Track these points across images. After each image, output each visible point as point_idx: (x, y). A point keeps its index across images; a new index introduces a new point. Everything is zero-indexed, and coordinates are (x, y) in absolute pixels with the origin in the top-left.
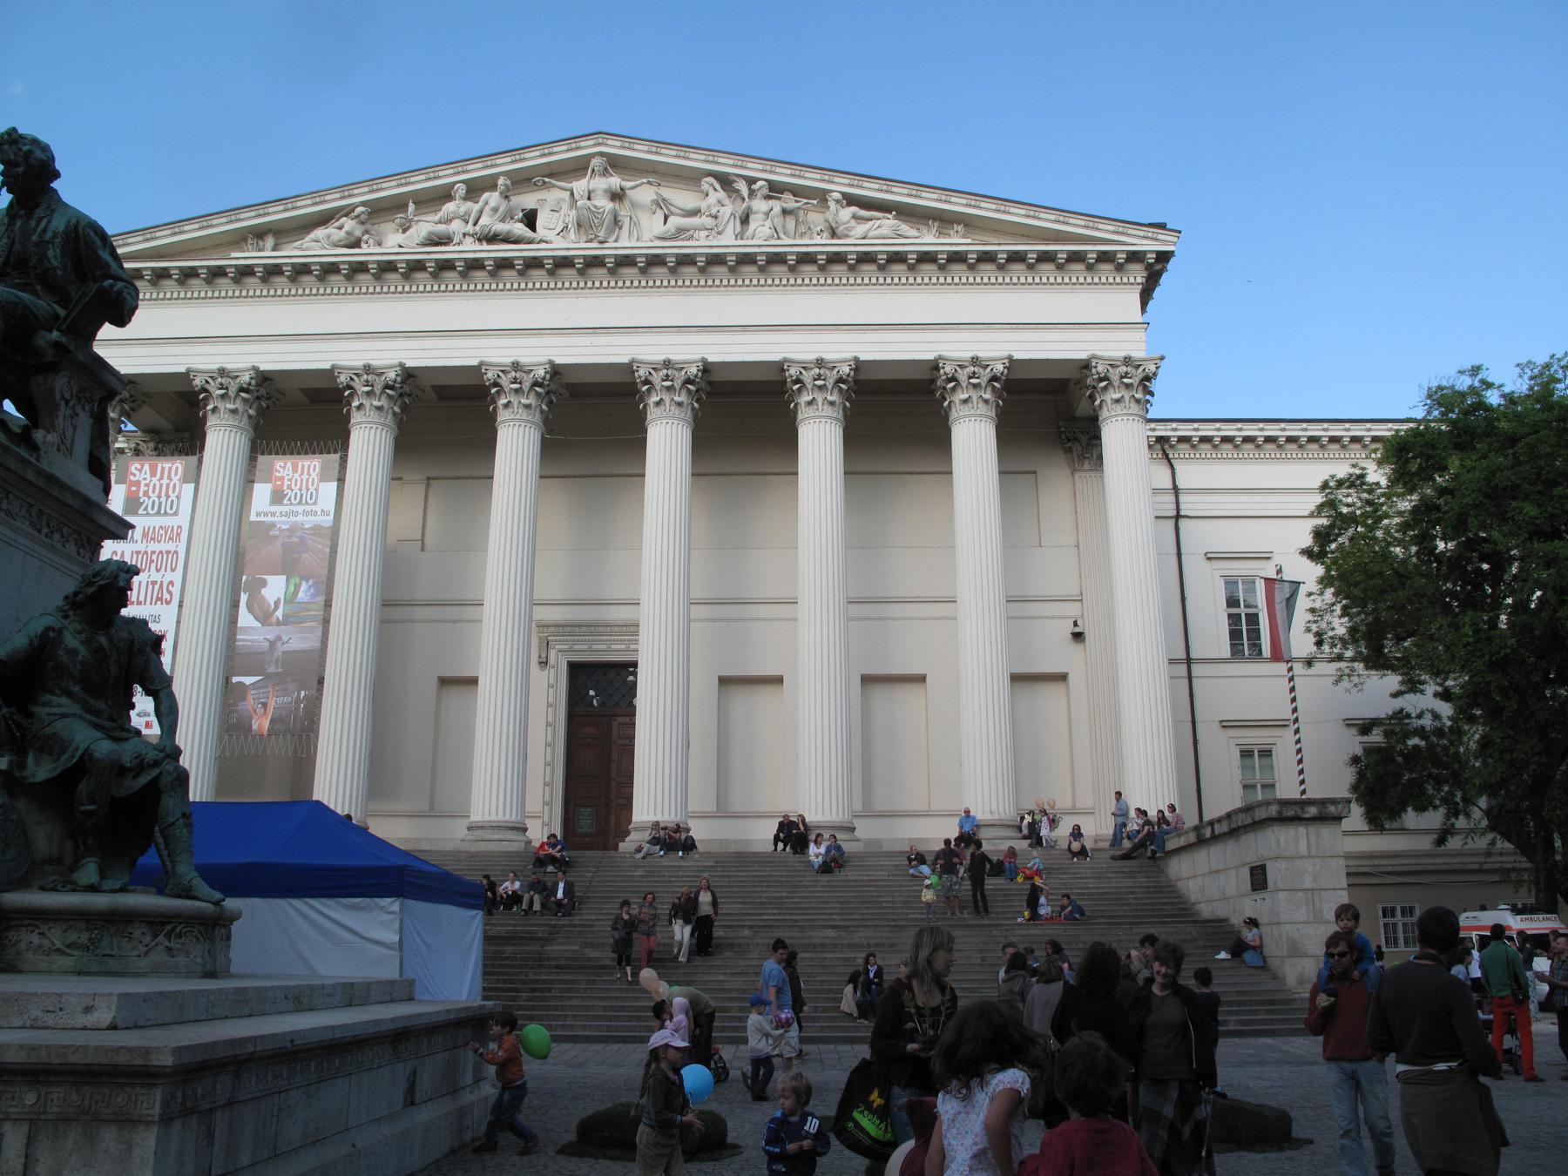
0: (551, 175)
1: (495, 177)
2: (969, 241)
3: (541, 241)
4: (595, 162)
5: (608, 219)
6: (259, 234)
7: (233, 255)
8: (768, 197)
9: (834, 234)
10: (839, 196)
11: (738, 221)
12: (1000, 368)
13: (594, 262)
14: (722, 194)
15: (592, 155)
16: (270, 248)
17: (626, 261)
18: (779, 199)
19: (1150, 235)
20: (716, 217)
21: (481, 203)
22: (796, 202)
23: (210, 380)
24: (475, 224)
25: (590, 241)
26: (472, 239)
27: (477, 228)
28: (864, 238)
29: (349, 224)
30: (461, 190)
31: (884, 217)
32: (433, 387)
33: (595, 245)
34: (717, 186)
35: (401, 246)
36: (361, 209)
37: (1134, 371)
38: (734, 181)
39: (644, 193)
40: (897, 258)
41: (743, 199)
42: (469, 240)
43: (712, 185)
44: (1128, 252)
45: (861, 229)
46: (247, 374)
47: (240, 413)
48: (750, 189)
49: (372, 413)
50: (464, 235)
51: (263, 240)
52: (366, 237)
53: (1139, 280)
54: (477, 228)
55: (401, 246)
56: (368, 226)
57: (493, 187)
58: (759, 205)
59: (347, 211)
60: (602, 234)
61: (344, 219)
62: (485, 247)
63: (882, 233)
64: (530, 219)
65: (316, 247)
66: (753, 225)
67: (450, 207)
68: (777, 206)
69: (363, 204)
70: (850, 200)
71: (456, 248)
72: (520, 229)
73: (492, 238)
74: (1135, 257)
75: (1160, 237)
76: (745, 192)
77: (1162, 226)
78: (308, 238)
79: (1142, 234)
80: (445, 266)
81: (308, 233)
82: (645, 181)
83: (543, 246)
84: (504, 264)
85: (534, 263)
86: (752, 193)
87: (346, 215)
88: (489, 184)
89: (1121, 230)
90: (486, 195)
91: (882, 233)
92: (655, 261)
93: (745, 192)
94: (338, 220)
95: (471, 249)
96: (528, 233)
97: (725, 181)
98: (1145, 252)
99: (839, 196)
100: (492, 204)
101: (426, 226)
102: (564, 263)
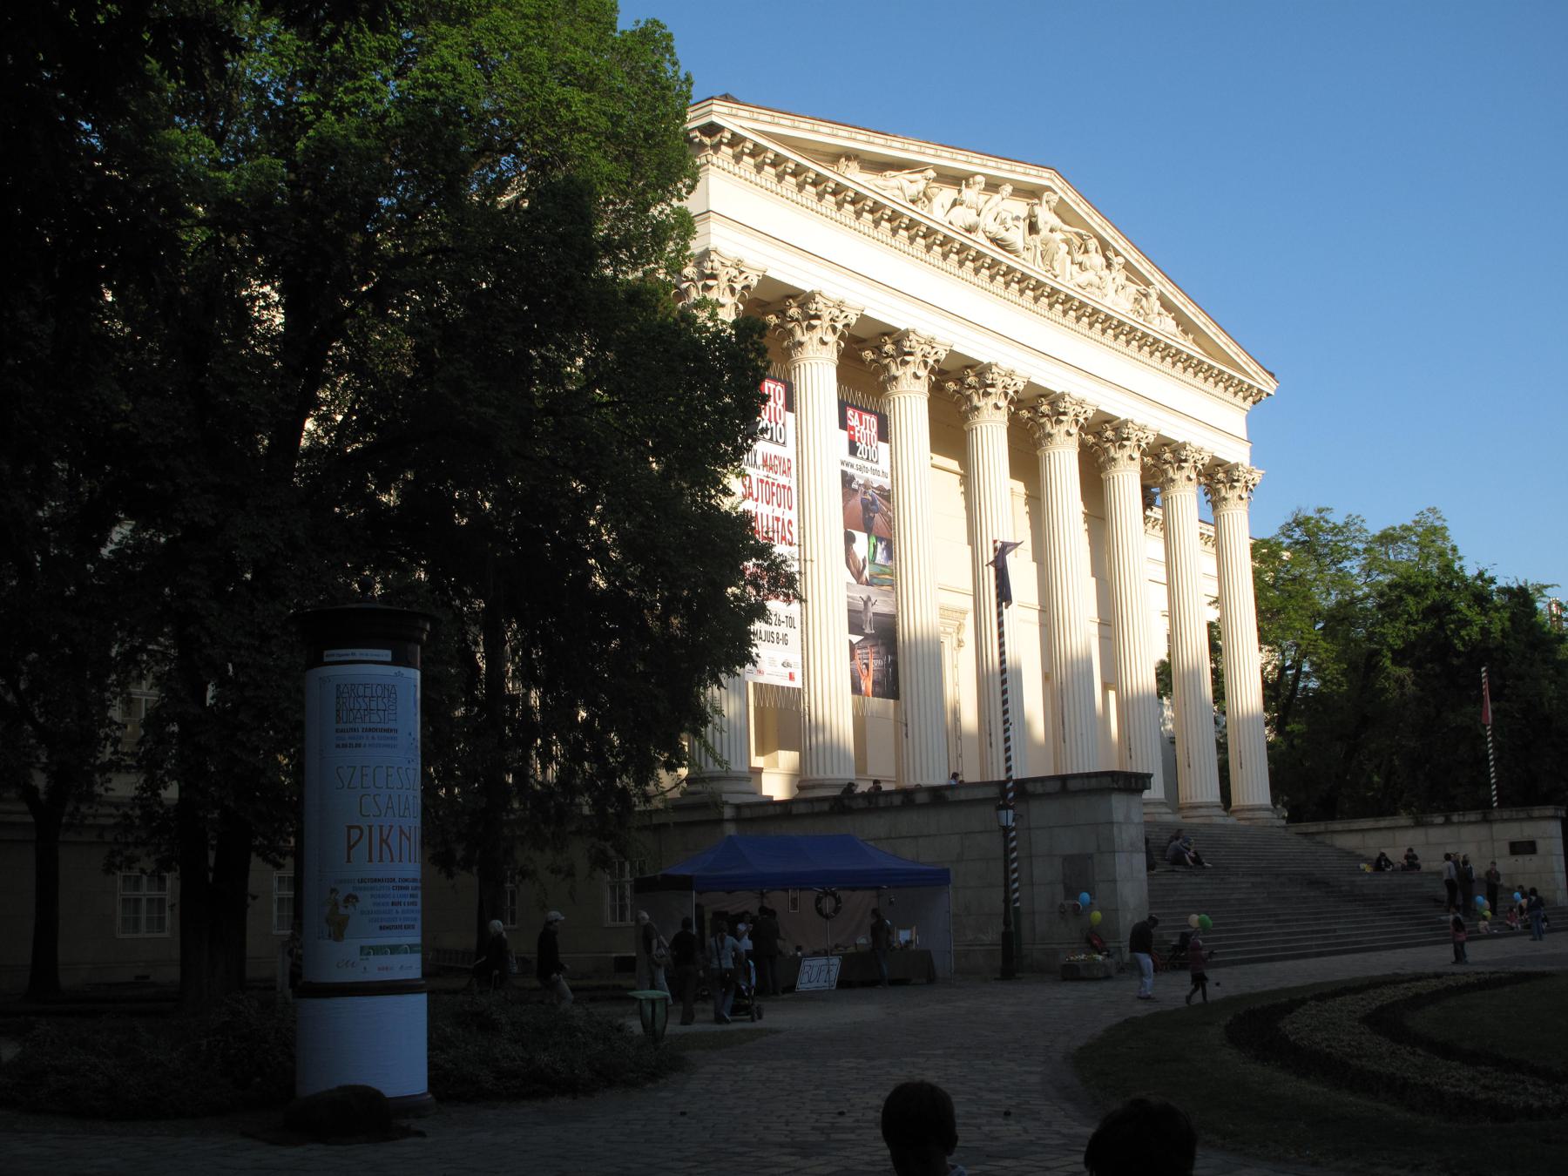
35: (950, 223)
55: (950, 223)
63: (1165, 327)
65: (892, 189)
69: (936, 168)
77: (1272, 375)
78: (894, 183)
91: (1165, 327)
97: (1104, 246)
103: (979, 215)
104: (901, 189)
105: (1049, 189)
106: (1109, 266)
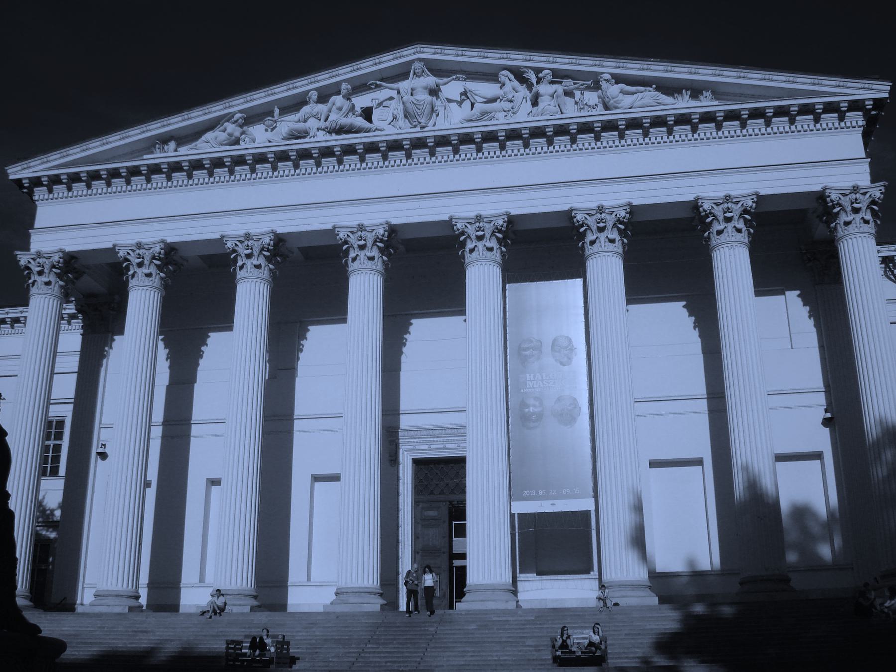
0: (382, 80)
1: (339, 84)
2: (716, 103)
3: (376, 129)
4: (417, 65)
5: (428, 109)
6: (164, 140)
7: (145, 157)
8: (552, 82)
9: (607, 107)
10: (608, 76)
11: (529, 102)
12: (750, 203)
13: (419, 144)
14: (516, 83)
15: (413, 61)
16: (172, 150)
17: (443, 141)
18: (561, 83)
19: (866, 86)
20: (511, 101)
21: (329, 104)
22: (575, 83)
23: (131, 252)
24: (326, 120)
25: (415, 127)
26: (324, 133)
27: (327, 124)
28: (630, 108)
29: (230, 127)
30: (314, 95)
31: (645, 90)
32: (301, 249)
33: (418, 129)
34: (512, 77)
35: (270, 142)
36: (238, 116)
37: (862, 197)
38: (525, 72)
39: (453, 88)
40: (659, 122)
41: (533, 85)
42: (321, 133)
43: (507, 76)
44: (850, 101)
45: (628, 100)
46: (158, 245)
47: (154, 276)
48: (537, 77)
49: (252, 270)
50: (318, 130)
51: (167, 145)
52: (244, 136)
53: (861, 123)
54: (327, 124)
55: (270, 142)
56: (245, 128)
57: (338, 93)
58: (544, 89)
59: (228, 118)
60: (422, 121)
61: (227, 124)
62: (334, 137)
64: (367, 114)
66: (541, 105)
67: (305, 109)
68: (559, 88)
69: (240, 111)
70: (618, 79)
71: (312, 140)
72: (360, 122)
73: (341, 130)
74: (855, 105)
75: (874, 86)
76: (534, 80)
79: (859, 85)
80: (305, 154)
81: (200, 137)
82: (454, 77)
83: (378, 133)
84: (350, 150)
85: (372, 148)
86: (539, 81)
87: (228, 121)
88: (335, 89)
89: (842, 83)
90: (333, 98)
92: (467, 139)
93: (534, 80)
94: (222, 126)
95: (322, 139)
96: (366, 124)
97: (519, 75)
98: (864, 100)
99: (608, 76)
100: (338, 104)
101: (288, 123)
102: (395, 146)
103: (320, 120)
104: (207, 142)
105: (420, 60)
106: (530, 86)
